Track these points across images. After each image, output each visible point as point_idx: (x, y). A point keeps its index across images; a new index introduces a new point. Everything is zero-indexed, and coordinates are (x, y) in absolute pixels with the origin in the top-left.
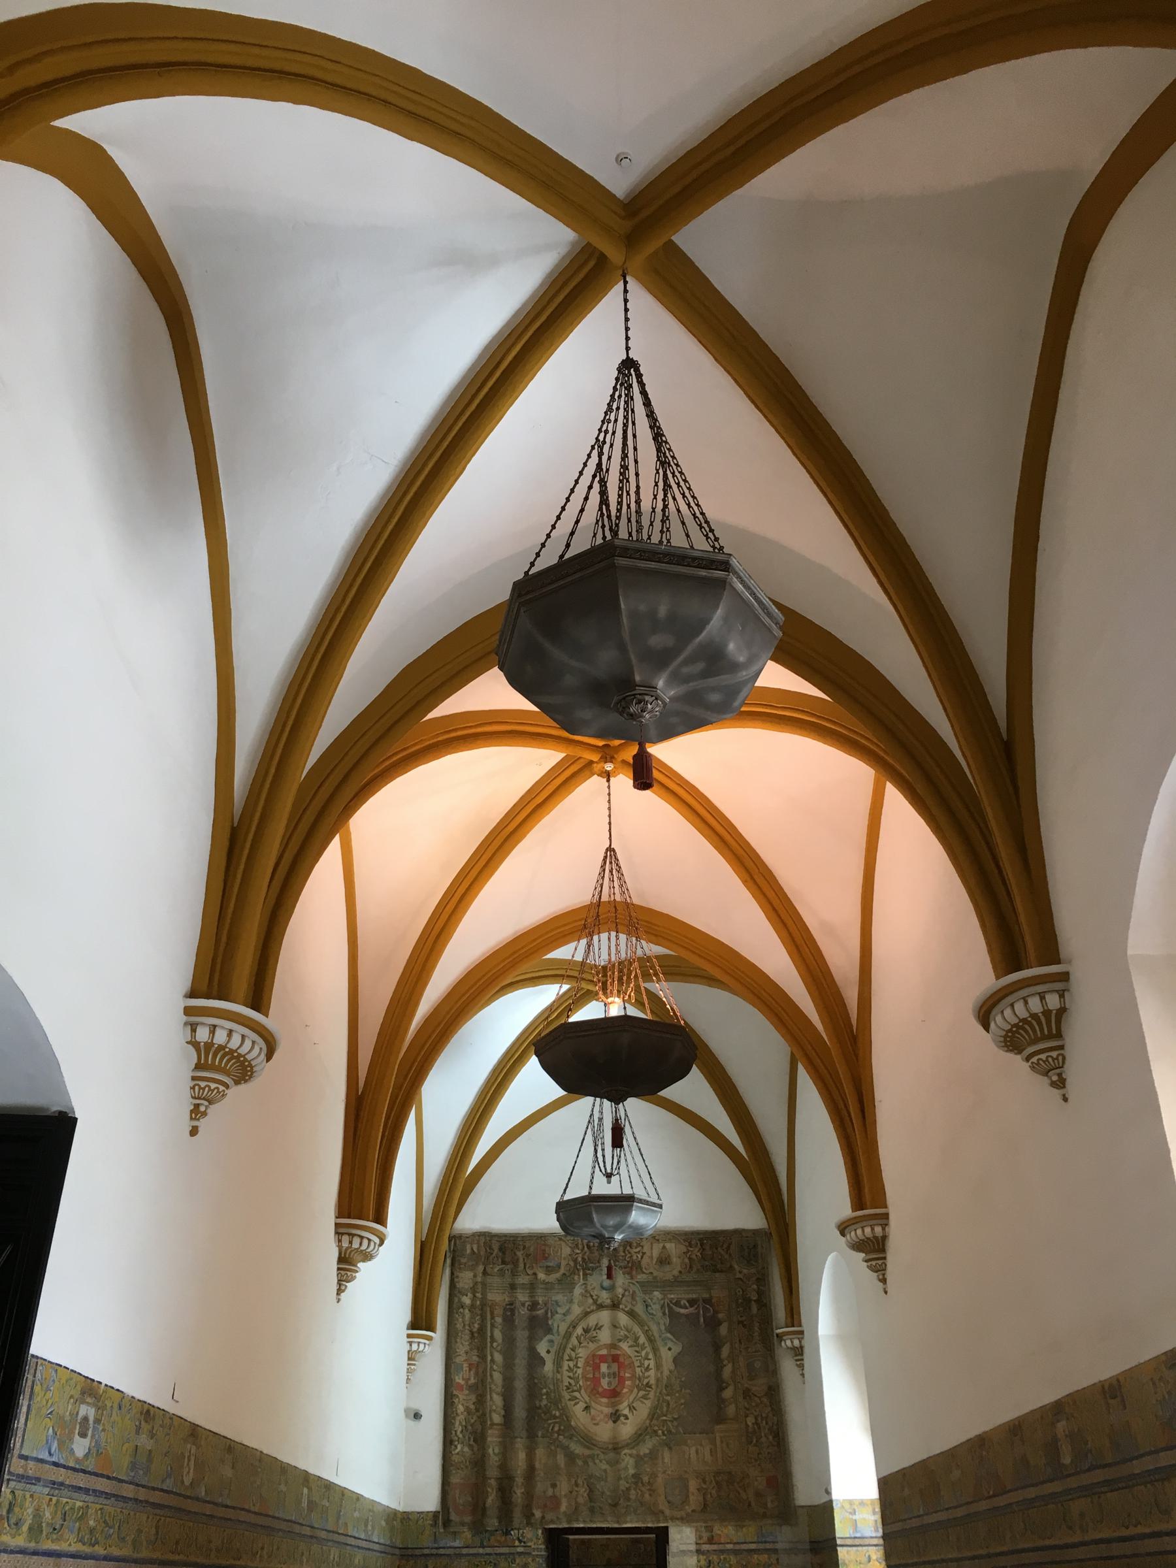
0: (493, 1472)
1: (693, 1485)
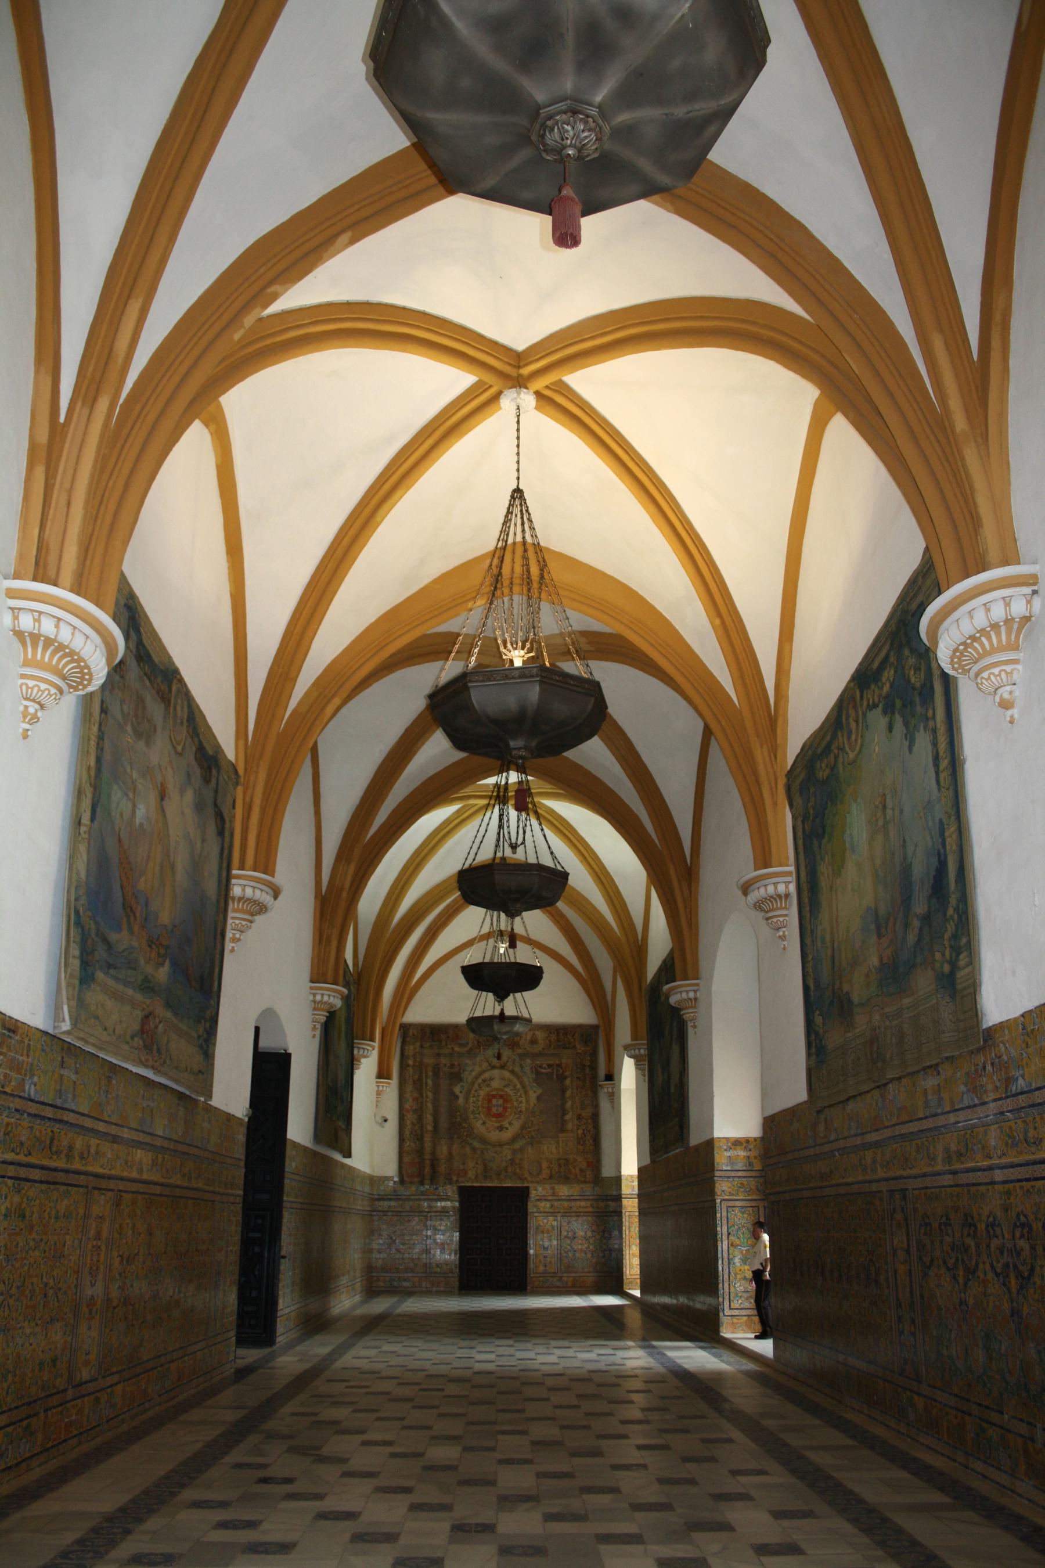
0: (427, 1156)
1: (545, 1165)
